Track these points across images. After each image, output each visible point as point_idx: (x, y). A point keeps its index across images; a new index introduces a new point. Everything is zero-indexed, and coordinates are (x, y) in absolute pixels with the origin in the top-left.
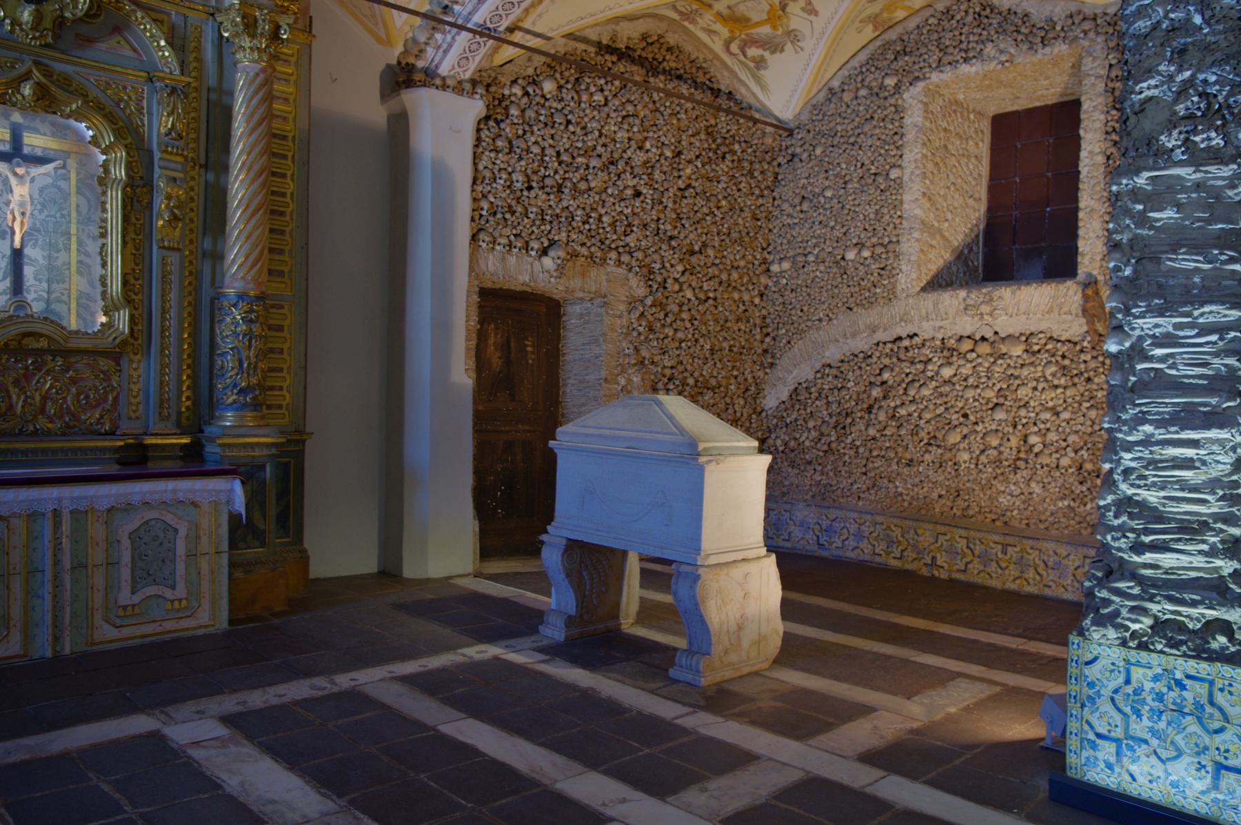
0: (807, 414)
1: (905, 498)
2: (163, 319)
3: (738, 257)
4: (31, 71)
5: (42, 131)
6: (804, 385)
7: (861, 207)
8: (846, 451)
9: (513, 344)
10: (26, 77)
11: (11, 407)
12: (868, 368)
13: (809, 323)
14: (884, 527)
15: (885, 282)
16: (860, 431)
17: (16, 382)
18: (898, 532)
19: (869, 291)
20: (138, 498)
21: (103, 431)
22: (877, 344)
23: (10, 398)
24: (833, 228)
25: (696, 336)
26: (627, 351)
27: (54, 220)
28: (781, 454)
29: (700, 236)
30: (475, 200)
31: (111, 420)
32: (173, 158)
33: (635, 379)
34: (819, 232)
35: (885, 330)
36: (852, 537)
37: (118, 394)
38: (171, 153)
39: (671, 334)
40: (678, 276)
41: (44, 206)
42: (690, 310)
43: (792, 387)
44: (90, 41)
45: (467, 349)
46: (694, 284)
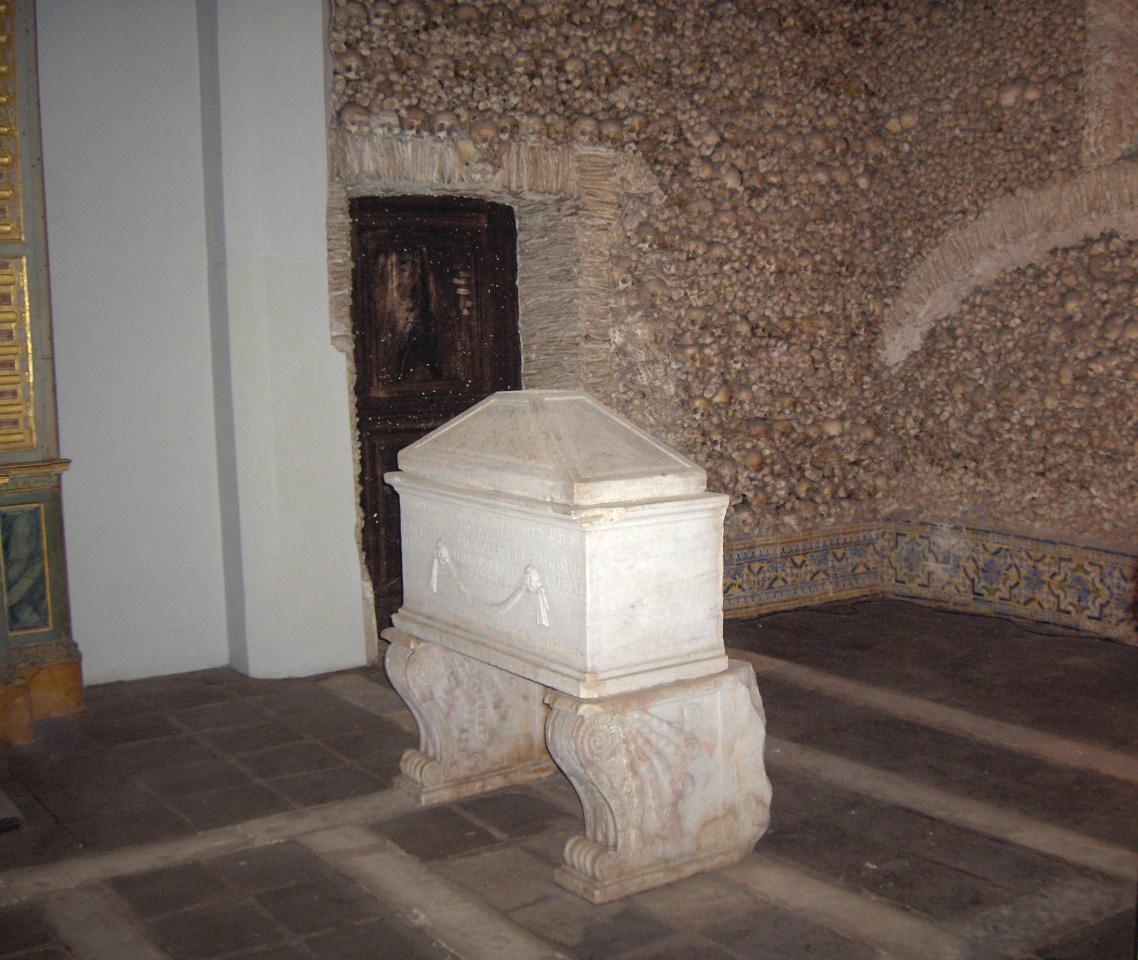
0: (951, 373)
1: (1106, 515)
3: (821, 112)
6: (945, 324)
7: (1021, 14)
8: (1012, 436)
9: (432, 286)
12: (1042, 294)
13: (948, 218)
14: (1073, 566)
15: (1064, 143)
16: (1034, 402)
18: (1094, 574)
19: (1038, 158)
22: (1053, 252)
24: (978, 53)
25: (749, 252)
26: (622, 286)
28: (914, 442)
29: (747, 80)
30: (337, 55)
33: (639, 332)
34: (956, 60)
35: (1067, 226)
36: (1023, 583)
39: (700, 252)
40: (708, 153)
42: (734, 209)
43: (926, 329)
45: (335, 303)
46: (740, 163)
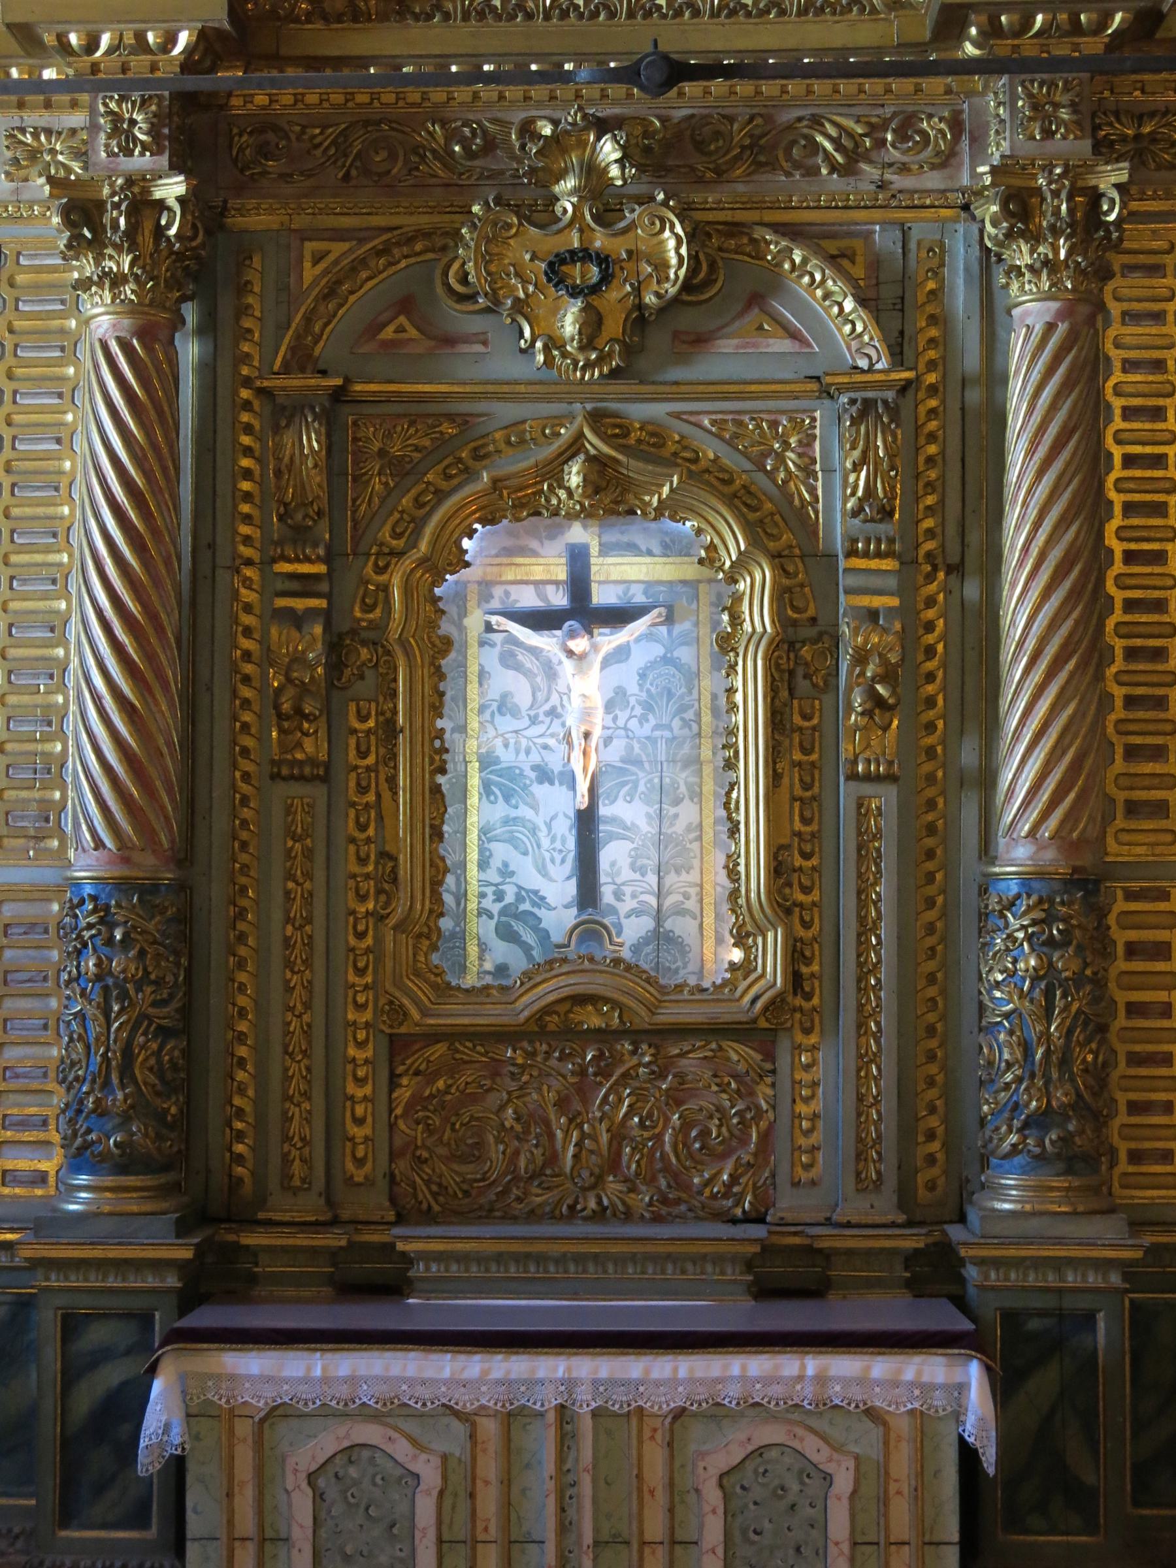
2: (862, 945)
4: (581, 435)
5: (644, 548)
10: (575, 447)
11: (553, 1158)
17: (562, 1104)
20: (734, 1391)
21: (738, 1212)
23: (551, 1136)
27: (667, 734)
31: (755, 1188)
32: (874, 564)
37: (771, 1126)
38: (866, 554)
41: (648, 707)
44: (700, 341)
